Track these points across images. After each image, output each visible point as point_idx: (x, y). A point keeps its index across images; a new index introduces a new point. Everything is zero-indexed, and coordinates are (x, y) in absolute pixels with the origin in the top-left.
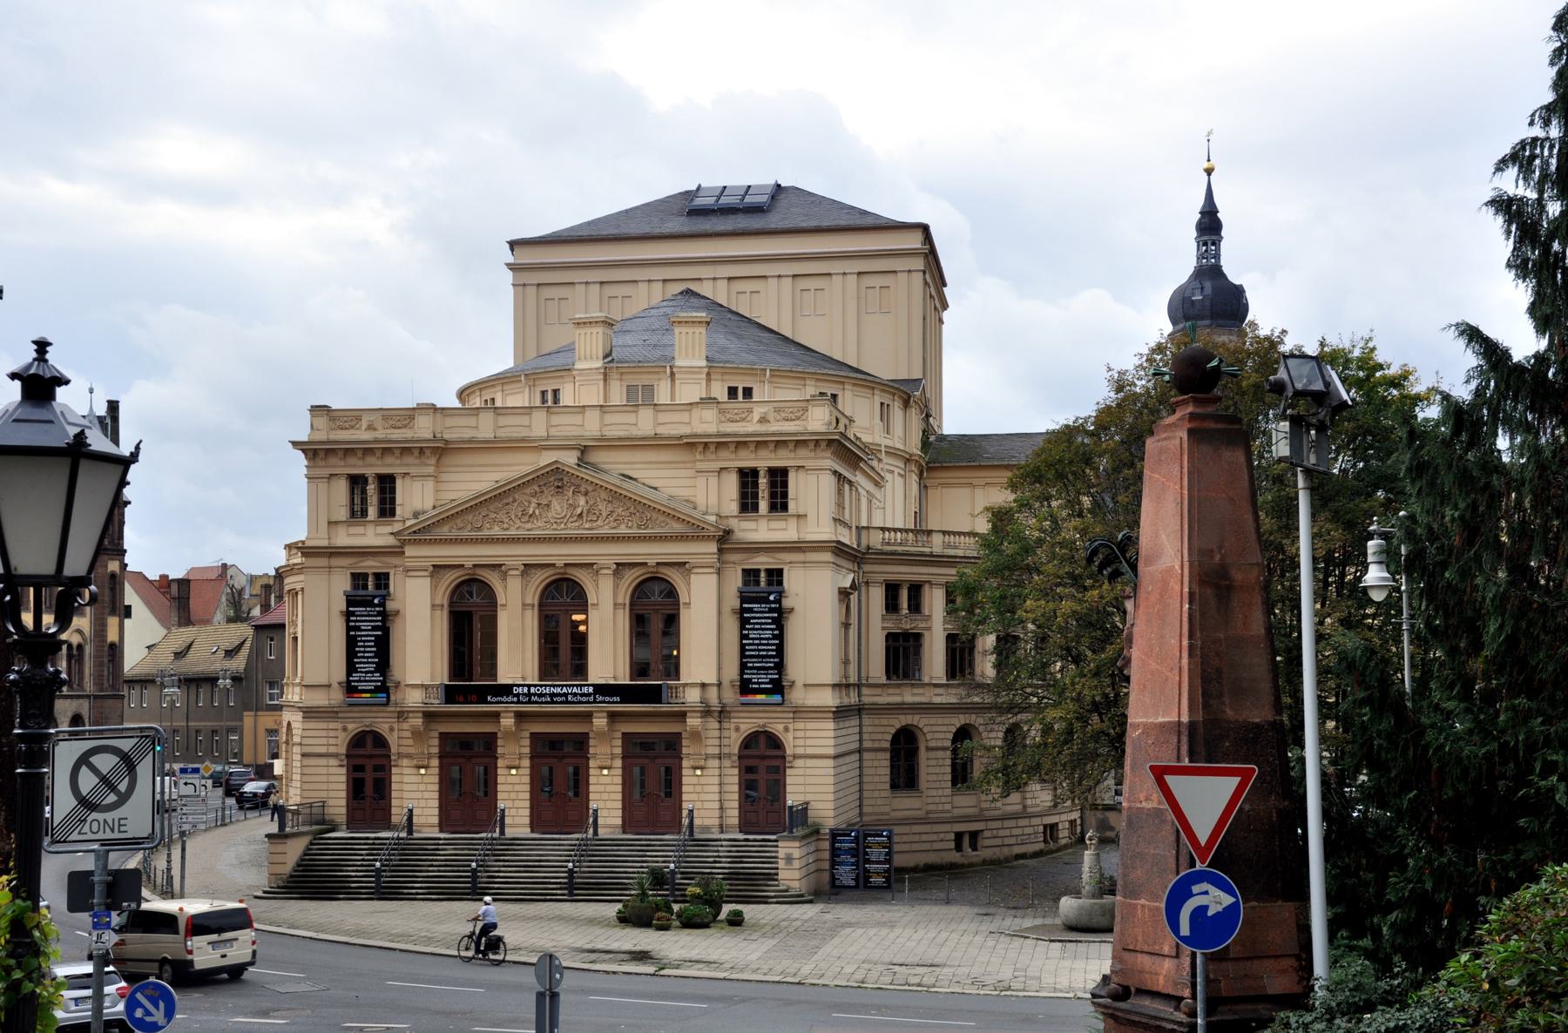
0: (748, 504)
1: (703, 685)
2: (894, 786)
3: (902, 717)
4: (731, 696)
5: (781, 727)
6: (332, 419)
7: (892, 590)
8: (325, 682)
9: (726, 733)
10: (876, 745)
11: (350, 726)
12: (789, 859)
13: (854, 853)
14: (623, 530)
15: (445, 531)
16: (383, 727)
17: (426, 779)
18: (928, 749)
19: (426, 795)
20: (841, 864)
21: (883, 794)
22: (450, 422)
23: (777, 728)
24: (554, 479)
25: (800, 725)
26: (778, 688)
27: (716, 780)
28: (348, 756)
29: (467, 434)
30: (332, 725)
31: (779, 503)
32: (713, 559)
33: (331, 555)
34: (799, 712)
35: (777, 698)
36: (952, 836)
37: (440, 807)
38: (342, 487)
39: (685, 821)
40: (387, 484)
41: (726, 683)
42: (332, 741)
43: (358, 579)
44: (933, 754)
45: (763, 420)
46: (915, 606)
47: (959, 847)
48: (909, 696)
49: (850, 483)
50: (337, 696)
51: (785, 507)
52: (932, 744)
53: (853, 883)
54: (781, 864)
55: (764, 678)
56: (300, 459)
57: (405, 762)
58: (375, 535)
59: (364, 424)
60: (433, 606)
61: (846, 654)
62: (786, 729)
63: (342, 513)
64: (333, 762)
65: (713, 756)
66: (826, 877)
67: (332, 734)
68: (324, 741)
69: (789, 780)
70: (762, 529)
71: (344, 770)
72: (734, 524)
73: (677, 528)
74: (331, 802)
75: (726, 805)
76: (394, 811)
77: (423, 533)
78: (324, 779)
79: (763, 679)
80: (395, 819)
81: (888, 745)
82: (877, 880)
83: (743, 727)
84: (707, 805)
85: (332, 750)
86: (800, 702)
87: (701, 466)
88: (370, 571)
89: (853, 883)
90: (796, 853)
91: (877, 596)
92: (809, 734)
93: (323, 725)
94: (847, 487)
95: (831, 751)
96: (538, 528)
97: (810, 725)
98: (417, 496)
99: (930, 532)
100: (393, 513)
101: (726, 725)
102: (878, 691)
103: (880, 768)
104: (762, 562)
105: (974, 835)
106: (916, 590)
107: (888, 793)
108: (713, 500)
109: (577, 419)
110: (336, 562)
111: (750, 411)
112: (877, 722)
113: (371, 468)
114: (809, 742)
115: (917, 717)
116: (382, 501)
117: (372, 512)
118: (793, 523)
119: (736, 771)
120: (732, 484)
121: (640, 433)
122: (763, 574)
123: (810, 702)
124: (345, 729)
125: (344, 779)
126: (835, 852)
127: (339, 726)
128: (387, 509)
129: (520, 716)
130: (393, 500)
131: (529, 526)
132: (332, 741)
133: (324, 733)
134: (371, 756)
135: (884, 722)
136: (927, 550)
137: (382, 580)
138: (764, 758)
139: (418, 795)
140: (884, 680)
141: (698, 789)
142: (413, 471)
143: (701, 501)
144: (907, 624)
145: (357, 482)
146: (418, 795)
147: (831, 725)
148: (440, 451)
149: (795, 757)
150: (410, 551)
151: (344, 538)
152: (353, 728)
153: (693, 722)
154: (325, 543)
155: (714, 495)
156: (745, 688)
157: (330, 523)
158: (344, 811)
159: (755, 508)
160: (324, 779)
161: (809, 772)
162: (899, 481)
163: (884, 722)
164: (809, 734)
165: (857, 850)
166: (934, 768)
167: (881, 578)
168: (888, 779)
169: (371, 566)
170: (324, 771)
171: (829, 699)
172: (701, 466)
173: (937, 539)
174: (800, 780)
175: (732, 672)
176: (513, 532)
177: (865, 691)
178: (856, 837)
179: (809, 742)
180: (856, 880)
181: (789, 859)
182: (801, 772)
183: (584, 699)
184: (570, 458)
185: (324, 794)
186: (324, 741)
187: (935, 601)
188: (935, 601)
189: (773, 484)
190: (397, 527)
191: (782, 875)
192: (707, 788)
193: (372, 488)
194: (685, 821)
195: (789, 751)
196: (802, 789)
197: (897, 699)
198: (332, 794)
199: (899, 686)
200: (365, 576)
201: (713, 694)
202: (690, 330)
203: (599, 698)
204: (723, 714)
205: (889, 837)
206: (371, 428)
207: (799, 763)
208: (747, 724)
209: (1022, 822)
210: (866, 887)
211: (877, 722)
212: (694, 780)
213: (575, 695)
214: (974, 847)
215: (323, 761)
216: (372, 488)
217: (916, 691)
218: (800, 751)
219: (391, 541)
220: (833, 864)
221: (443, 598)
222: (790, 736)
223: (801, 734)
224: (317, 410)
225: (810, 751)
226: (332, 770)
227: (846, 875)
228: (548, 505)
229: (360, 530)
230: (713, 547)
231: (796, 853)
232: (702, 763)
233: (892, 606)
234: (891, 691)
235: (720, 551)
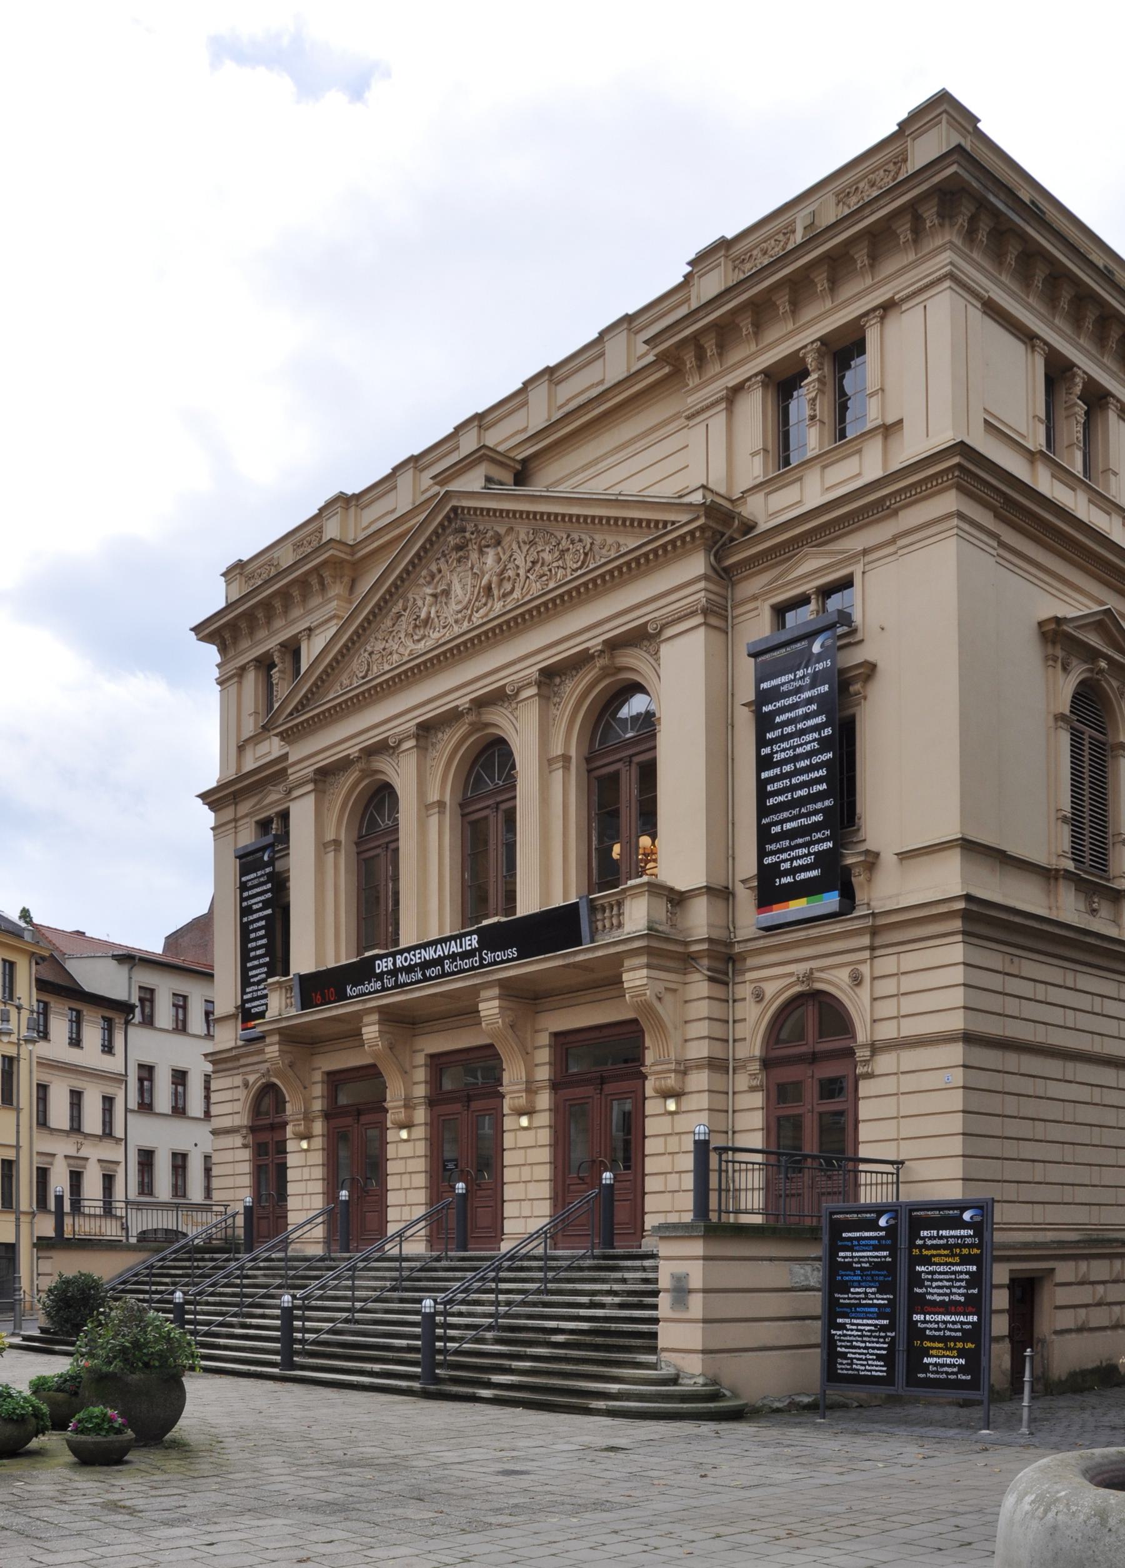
5: (843, 976)
9: (741, 1010)
11: (251, 1078)
13: (883, 1276)
20: (852, 1310)
23: (836, 981)
25: (887, 964)
26: (838, 877)
34: (882, 931)
35: (830, 901)
53: (878, 1369)
55: (803, 856)
66: (815, 1358)
69: (865, 1110)
79: (798, 859)
82: (942, 1361)
83: (770, 989)
86: (878, 906)
89: (878, 1369)
90: (696, 1275)
92: (908, 983)
95: (956, 1022)
114: (909, 1005)
119: (758, 1099)
124: (246, 1085)
126: (836, 1279)
127: (238, 1081)
129: (391, 1017)
138: (814, 1058)
147: (956, 951)
149: (876, 1048)
153: (635, 978)
156: (770, 889)
164: (908, 983)
165: (890, 1268)
171: (946, 879)
174: (887, 1107)
178: (891, 1230)
180: (888, 1359)
181: (681, 1291)
183: (466, 964)
195: (862, 1035)
201: (700, 920)
203: (489, 957)
204: (725, 962)
205: (978, 1227)
207: (885, 1062)
208: (772, 980)
210: (912, 1381)
213: (453, 957)
218: (888, 1031)
220: (833, 1313)
222: (865, 993)
223: (887, 987)
227: (864, 1345)
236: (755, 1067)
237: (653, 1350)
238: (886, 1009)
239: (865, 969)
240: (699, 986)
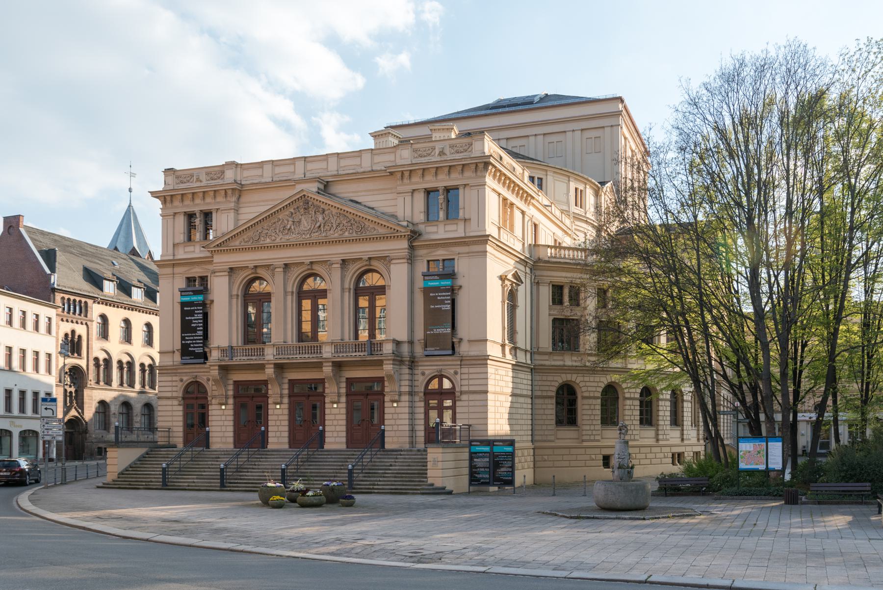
1: (398, 343)
2: (559, 422)
3: (563, 376)
4: (419, 350)
5: (452, 371)
6: (177, 177)
8: (170, 349)
9: (416, 377)
10: (545, 394)
11: (185, 378)
15: (236, 243)
16: (203, 379)
17: (226, 412)
18: (584, 398)
19: (226, 423)
21: (550, 427)
22: (246, 173)
24: (304, 203)
25: (465, 370)
27: (407, 410)
28: (183, 398)
30: (175, 378)
32: (405, 253)
37: (235, 432)
38: (181, 221)
40: (207, 215)
41: (416, 340)
42: (175, 389)
43: (190, 280)
44: (586, 401)
45: (442, 153)
46: (575, 300)
48: (569, 360)
50: (177, 357)
52: (586, 394)
54: (429, 465)
56: (158, 203)
57: (214, 401)
60: (231, 296)
62: (456, 373)
63: (181, 238)
64: (176, 402)
65: (405, 393)
67: (174, 384)
68: (170, 389)
70: (440, 231)
71: (181, 408)
72: (421, 228)
75: (417, 428)
77: (224, 245)
78: (170, 414)
81: (554, 394)
83: (427, 372)
84: (401, 428)
85: (175, 394)
86: (465, 354)
87: (401, 189)
88: (197, 275)
92: (471, 376)
93: (169, 378)
96: (293, 237)
97: (472, 370)
98: (223, 224)
101: (416, 372)
102: (546, 357)
103: (550, 409)
104: (441, 254)
107: (553, 427)
108: (408, 213)
110: (178, 270)
111: (434, 149)
112: (544, 378)
113: (197, 206)
114: (471, 382)
115: (574, 376)
118: (461, 225)
120: (420, 198)
121: (362, 170)
123: (472, 353)
124: (181, 380)
125: (181, 413)
127: (177, 378)
131: (287, 237)
132: (175, 389)
133: (170, 384)
134: (197, 398)
135: (550, 378)
137: (204, 279)
139: (221, 423)
140: (550, 350)
141: (395, 416)
142: (222, 207)
143: (400, 214)
144: (567, 311)
146: (221, 423)
148: (239, 191)
150: (217, 259)
151: (181, 254)
152: (187, 379)
153: (388, 367)
154: (171, 258)
155: (408, 207)
157: (174, 245)
160: (170, 414)
161: (471, 403)
163: (550, 378)
164: (471, 376)
166: (589, 410)
167: (548, 280)
169: (197, 272)
170: (170, 408)
172: (401, 189)
175: (420, 334)
177: (536, 357)
179: (471, 382)
182: (466, 403)
184: (313, 187)
185: (170, 424)
186: (170, 389)
191: (430, 473)
192: (401, 416)
193: (198, 221)
196: (466, 416)
197: (561, 363)
198: (175, 424)
199: (563, 355)
206: (198, 180)
207: (464, 397)
211: (544, 378)
212: (392, 411)
215: (169, 402)
216: (198, 221)
217: (575, 358)
218: (465, 389)
221: (237, 289)
223: (466, 376)
224: (168, 171)
225: (472, 388)
226: (175, 408)
228: (299, 222)
229: (191, 249)
230: (404, 244)
231: (440, 457)
232: (397, 398)
233: (557, 299)
234: (555, 358)
235: (412, 248)
236: (422, 394)
237: (426, 478)
238: (465, 382)
239: (459, 371)
240: (406, 370)
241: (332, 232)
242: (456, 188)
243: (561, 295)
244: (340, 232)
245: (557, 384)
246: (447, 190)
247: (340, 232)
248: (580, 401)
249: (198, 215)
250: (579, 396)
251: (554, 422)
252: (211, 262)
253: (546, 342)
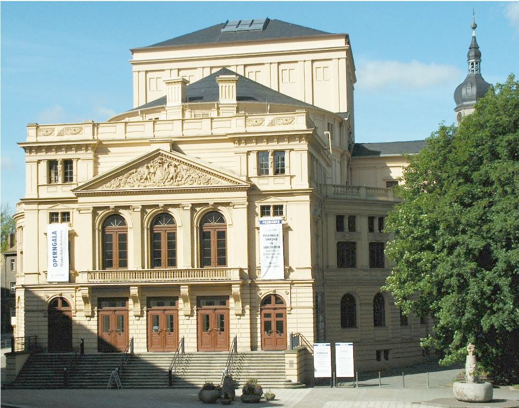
0: (262, 171)
7: (340, 219)
12: (291, 364)
14: (195, 185)
29: (110, 137)
31: (279, 170)
33: (40, 203)
36: (375, 352)
39: (232, 344)
40: (68, 163)
46: (352, 228)
47: (378, 358)
49: (317, 161)
51: (283, 171)
54: (287, 366)
58: (63, 191)
59: (56, 132)
61: (317, 251)
63: (43, 180)
64: (41, 314)
71: (46, 319)
72: (255, 181)
73: (225, 183)
74: (40, 336)
76: (74, 341)
77: (88, 189)
80: (74, 345)
88: (60, 211)
91: (332, 222)
94: (315, 163)
96: (149, 185)
98: (83, 172)
99: (359, 188)
100: (71, 179)
105: (386, 352)
106: (352, 219)
109: (169, 126)
110: (41, 207)
111: (263, 120)
113: (60, 156)
116: (66, 174)
117: (60, 179)
122: (271, 208)
128: (68, 177)
130: (71, 173)
131: (143, 184)
136: (357, 197)
138: (275, 309)
144: (347, 236)
145: (52, 164)
150: (80, 199)
151: (45, 193)
158: (47, 341)
159: (267, 172)
161: (299, 316)
162: (338, 165)
168: (340, 321)
170: (36, 319)
173: (363, 192)
176: (136, 187)
184: (166, 147)
187: (362, 224)
188: (362, 224)
189: (275, 161)
190: (75, 187)
191: (287, 372)
194: (232, 344)
200: (57, 214)
202: (227, 85)
209: (410, 345)
214: (387, 359)
215: (36, 314)
219: (72, 195)
230: (244, 194)
233: (340, 228)
241: (183, 182)
242: (283, 151)
243: (342, 222)
244: (191, 182)
245: (342, 295)
246: (275, 152)
247: (191, 182)
248: (358, 307)
249: (59, 162)
250: (358, 302)
251: (340, 325)
252: (76, 202)
253: (333, 260)
